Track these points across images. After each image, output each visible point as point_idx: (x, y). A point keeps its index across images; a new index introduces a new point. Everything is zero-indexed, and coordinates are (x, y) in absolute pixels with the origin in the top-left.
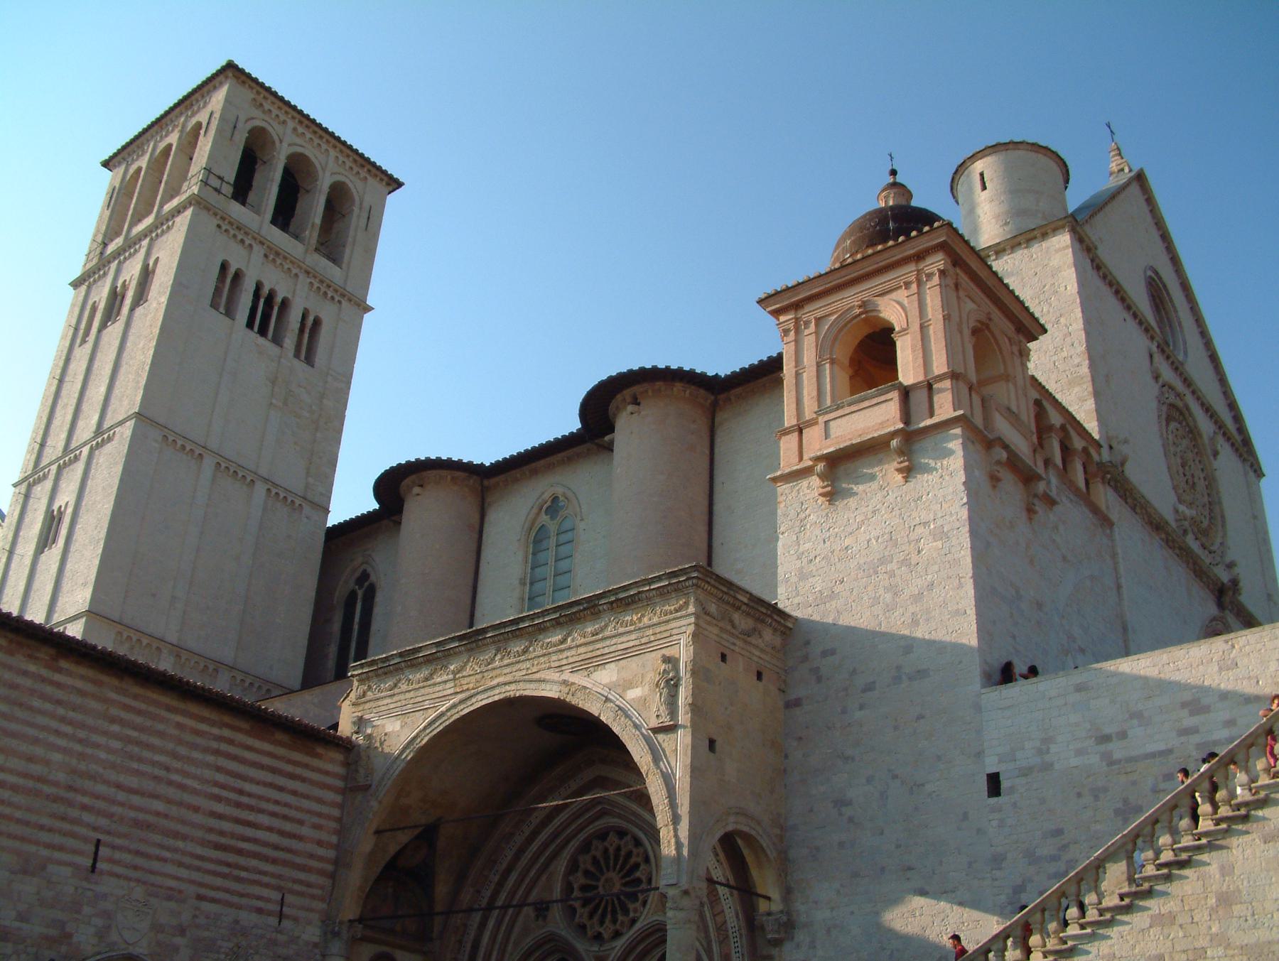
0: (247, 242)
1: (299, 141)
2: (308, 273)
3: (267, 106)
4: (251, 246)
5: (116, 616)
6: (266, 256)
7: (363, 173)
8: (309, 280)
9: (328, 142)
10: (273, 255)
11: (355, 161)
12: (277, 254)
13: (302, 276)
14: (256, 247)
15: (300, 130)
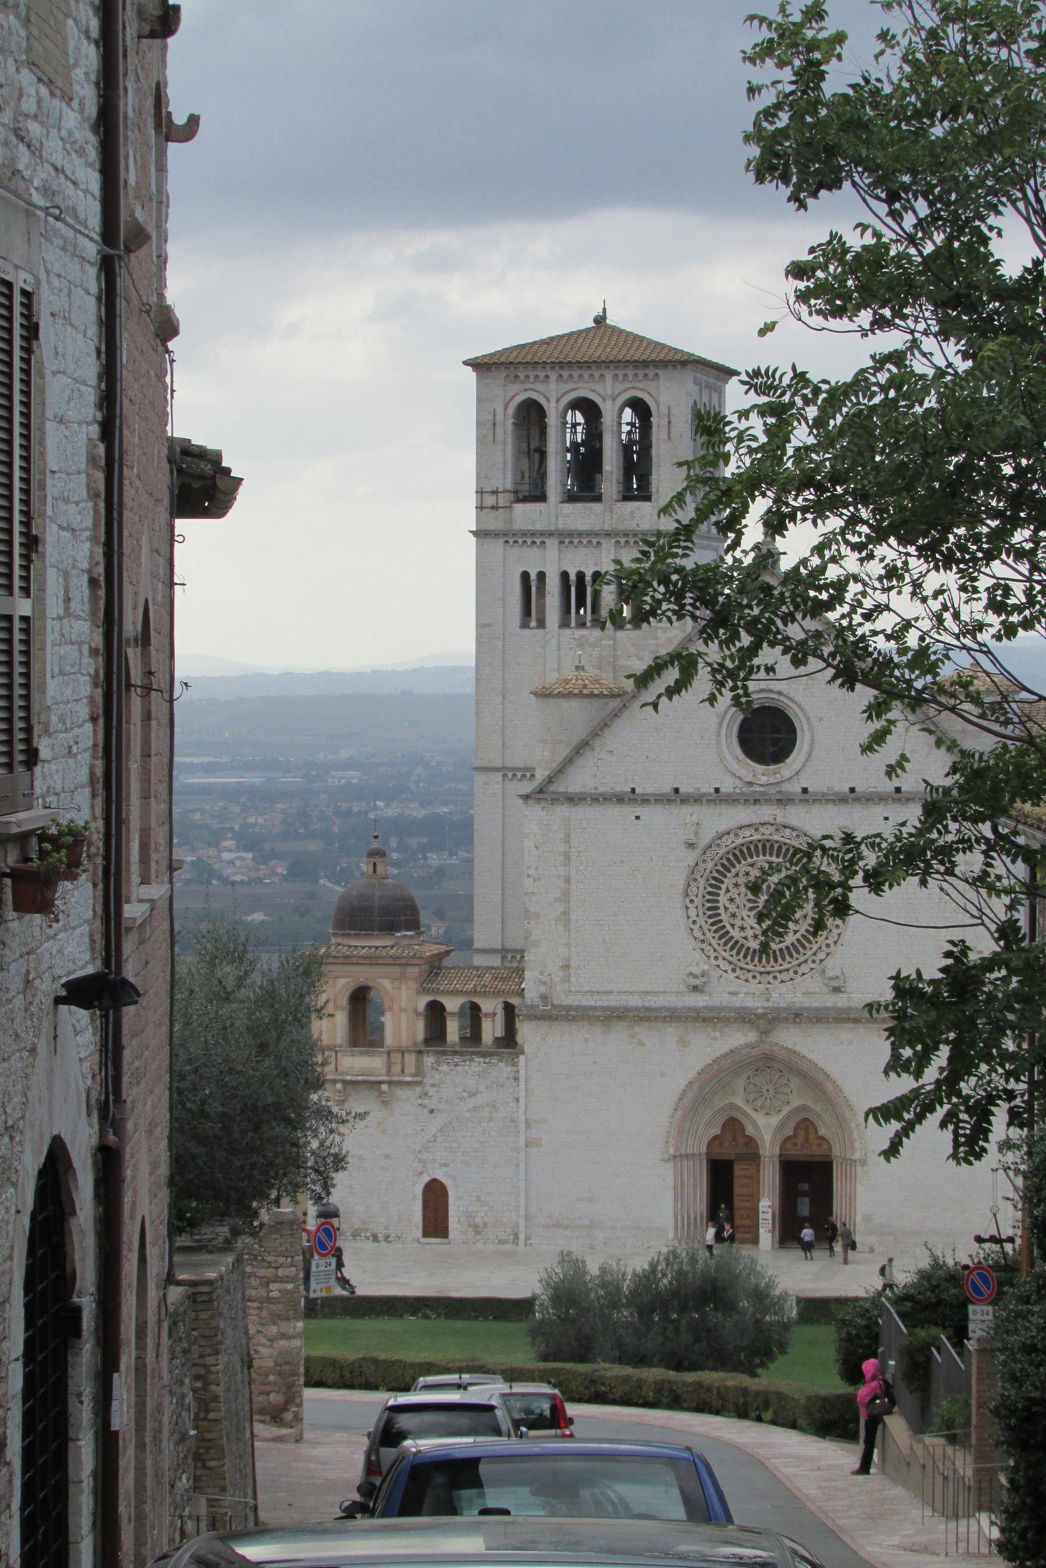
0: (538, 541)
1: (570, 386)
2: (608, 535)
3: (522, 377)
4: (543, 542)
5: (499, 946)
6: (562, 542)
7: (651, 374)
8: (613, 541)
9: (598, 368)
10: (567, 537)
11: (636, 367)
12: (571, 534)
13: (604, 541)
14: (548, 542)
15: (565, 374)
